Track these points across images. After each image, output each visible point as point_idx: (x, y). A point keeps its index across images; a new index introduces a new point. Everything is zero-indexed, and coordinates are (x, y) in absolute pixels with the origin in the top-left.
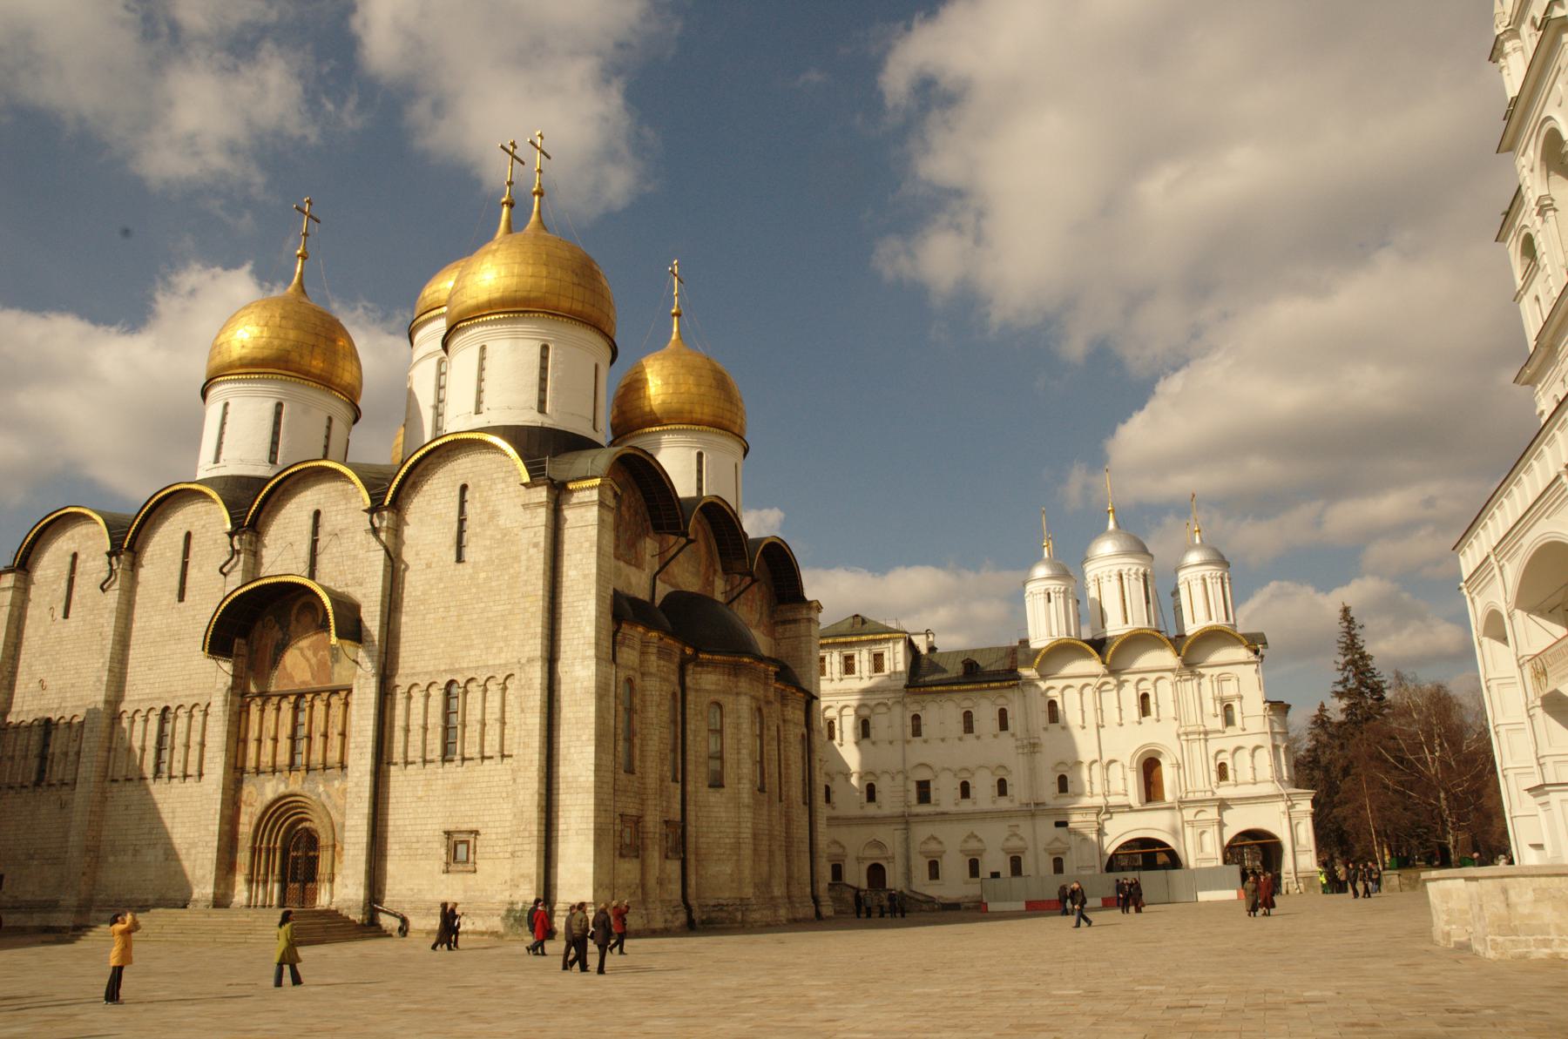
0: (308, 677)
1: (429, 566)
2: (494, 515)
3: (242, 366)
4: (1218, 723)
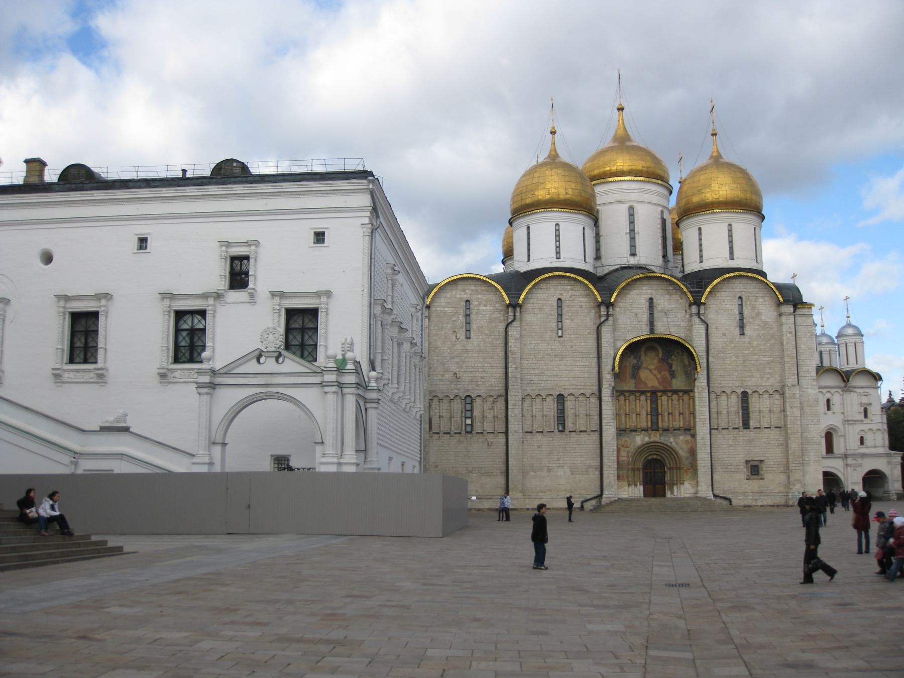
0: (656, 384)
1: (724, 335)
2: (758, 314)
4: (862, 416)
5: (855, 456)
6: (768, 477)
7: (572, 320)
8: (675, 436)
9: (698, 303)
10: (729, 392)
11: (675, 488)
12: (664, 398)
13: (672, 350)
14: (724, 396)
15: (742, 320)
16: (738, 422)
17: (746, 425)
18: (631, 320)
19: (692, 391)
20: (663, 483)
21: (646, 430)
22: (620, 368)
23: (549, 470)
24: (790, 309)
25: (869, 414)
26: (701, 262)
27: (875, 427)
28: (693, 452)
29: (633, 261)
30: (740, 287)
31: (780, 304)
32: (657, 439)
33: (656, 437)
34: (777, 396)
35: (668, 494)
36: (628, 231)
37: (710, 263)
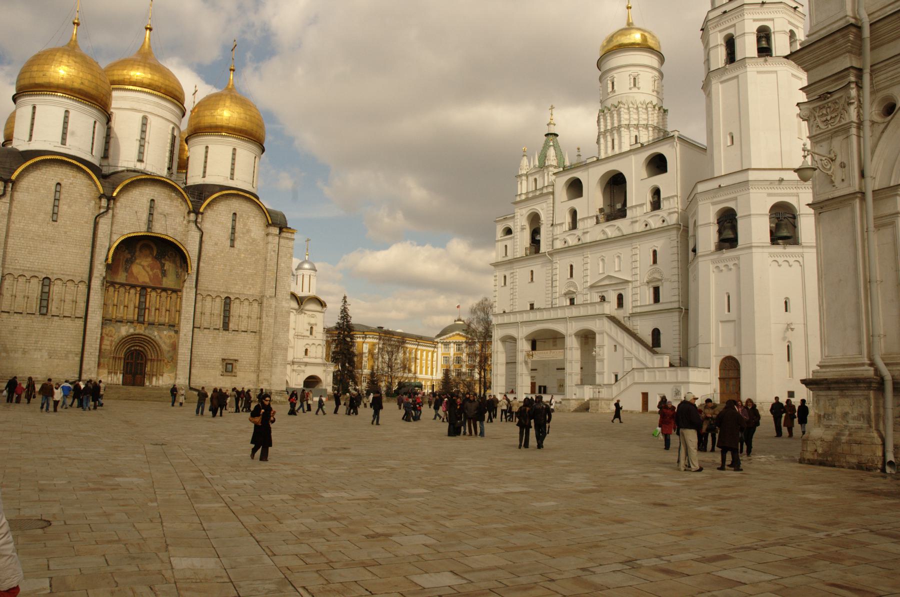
0: (147, 280)
1: (216, 244)
2: (249, 231)
3: (79, 93)
5: (300, 363)
6: (240, 374)
7: (70, 207)
8: (159, 330)
9: (197, 213)
10: (214, 296)
11: (154, 379)
12: (154, 294)
13: (167, 250)
14: (209, 299)
15: (233, 233)
16: (219, 323)
17: (226, 327)
18: (131, 216)
19: (180, 291)
20: (143, 374)
21: (132, 322)
22: (113, 260)
23: (24, 352)
24: (276, 231)
25: (314, 333)
26: (204, 177)
27: (317, 342)
28: (174, 347)
29: (140, 166)
30: (236, 205)
31: (268, 225)
32: (142, 332)
33: (140, 330)
34: (256, 305)
35: (147, 383)
36: (139, 138)
37: (209, 180)
